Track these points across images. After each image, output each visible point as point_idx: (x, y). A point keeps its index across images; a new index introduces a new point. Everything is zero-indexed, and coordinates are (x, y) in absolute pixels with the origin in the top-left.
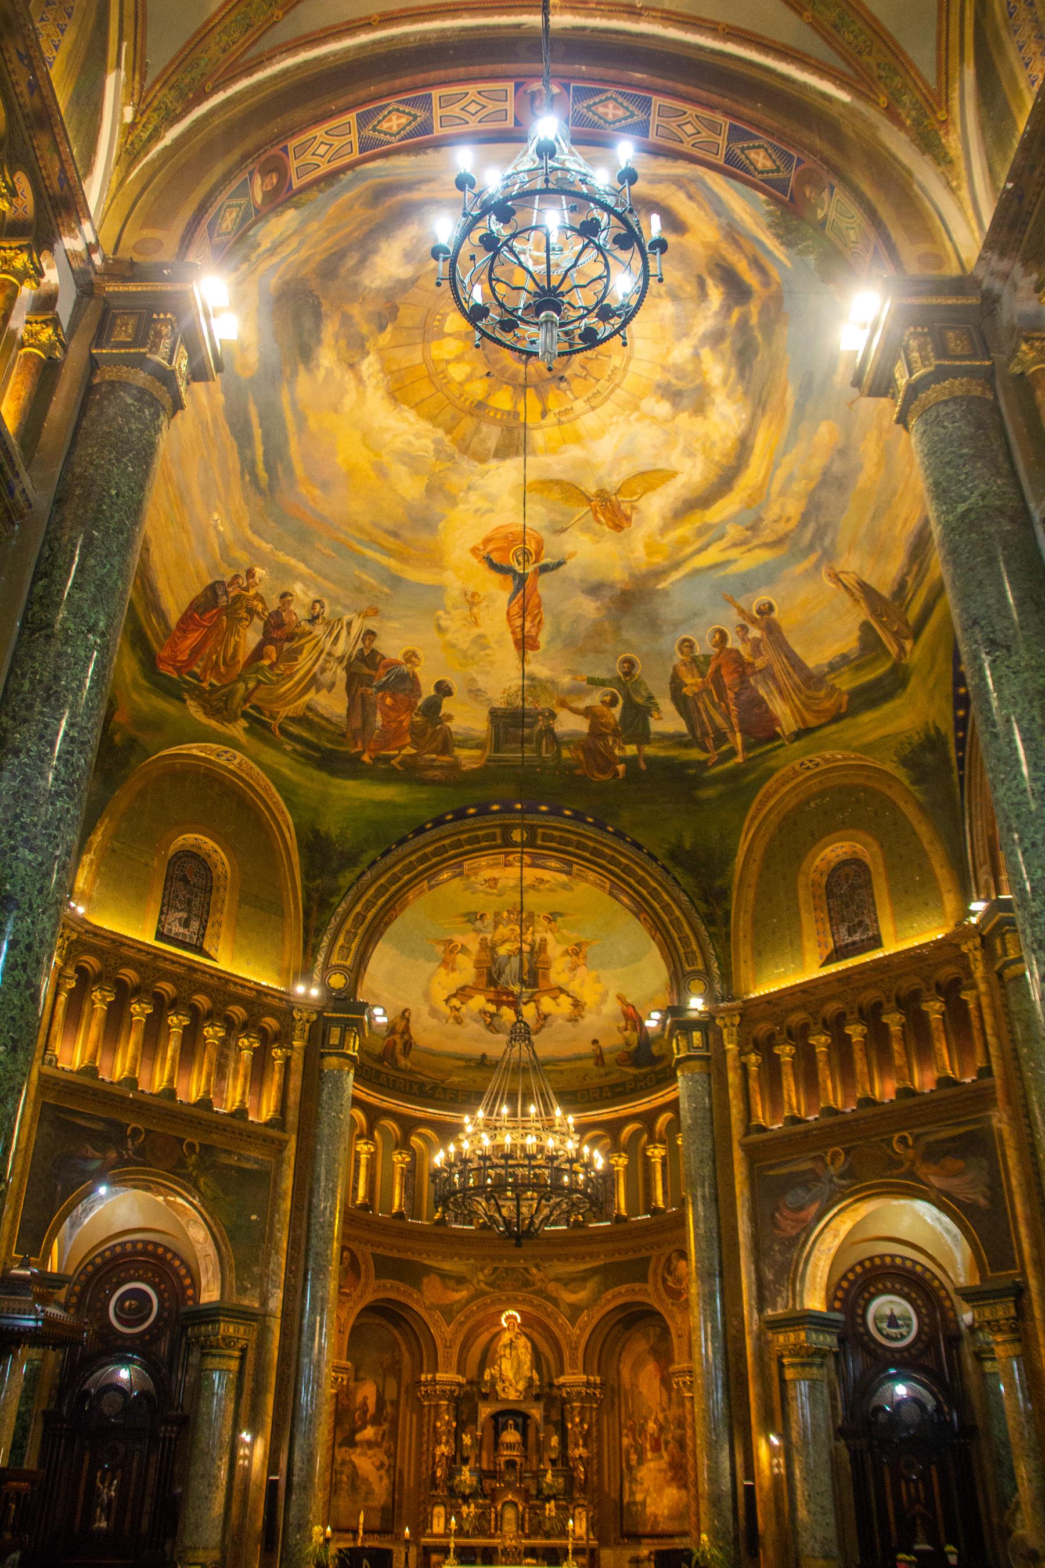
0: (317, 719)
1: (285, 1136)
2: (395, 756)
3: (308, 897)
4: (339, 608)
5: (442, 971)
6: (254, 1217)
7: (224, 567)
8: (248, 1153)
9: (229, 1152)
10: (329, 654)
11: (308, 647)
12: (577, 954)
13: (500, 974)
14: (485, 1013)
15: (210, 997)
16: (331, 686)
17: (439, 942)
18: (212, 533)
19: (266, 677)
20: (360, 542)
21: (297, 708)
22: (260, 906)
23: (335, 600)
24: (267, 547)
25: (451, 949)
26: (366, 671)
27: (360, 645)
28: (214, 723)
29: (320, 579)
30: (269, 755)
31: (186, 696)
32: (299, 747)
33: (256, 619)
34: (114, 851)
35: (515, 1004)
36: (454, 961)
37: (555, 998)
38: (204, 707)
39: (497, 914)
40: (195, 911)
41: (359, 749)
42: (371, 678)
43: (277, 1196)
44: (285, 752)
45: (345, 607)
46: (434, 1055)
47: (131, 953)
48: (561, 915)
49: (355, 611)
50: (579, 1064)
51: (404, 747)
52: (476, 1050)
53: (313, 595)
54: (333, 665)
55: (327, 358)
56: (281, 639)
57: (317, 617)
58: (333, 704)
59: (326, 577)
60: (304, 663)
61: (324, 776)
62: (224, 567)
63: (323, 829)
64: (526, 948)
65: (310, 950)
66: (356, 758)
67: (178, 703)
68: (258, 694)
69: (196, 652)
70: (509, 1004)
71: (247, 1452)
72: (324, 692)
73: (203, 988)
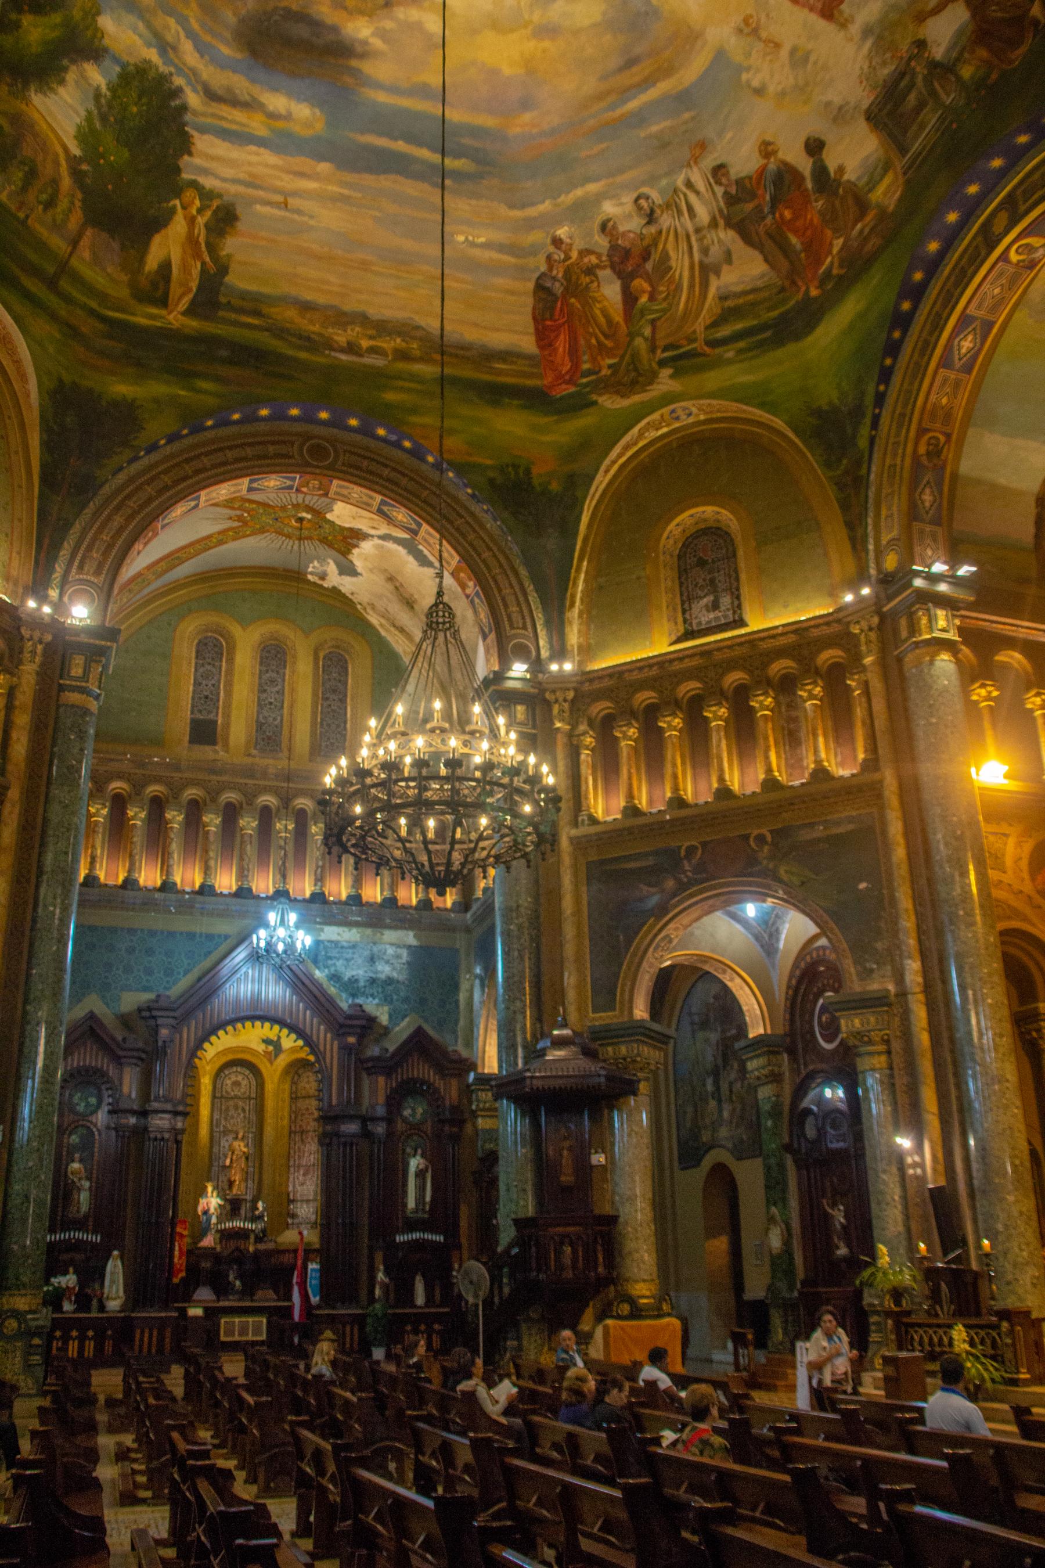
0: (741, 301)
1: (877, 776)
2: (832, 263)
3: (841, 486)
4: (664, 182)
6: (863, 886)
7: (531, 262)
8: (836, 816)
9: (812, 825)
10: (698, 230)
11: (670, 246)
15: (743, 668)
16: (728, 257)
18: (477, 252)
19: (657, 311)
20: (612, 107)
21: (711, 308)
22: (785, 536)
23: (652, 180)
24: (546, 206)
26: (749, 207)
27: (719, 191)
28: (636, 398)
29: (619, 179)
30: (713, 379)
31: (594, 397)
32: (741, 344)
33: (601, 273)
34: (601, 588)
38: (617, 392)
40: (721, 586)
41: (803, 289)
42: (759, 209)
43: (887, 848)
44: (730, 362)
45: (668, 174)
47: (636, 676)
49: (683, 167)
51: (831, 245)
53: (628, 199)
54: (711, 236)
55: (361, 30)
56: (639, 266)
57: (652, 211)
58: (746, 270)
59: (621, 171)
60: (681, 265)
61: (792, 347)
62: (531, 262)
63: (823, 403)
65: (857, 544)
66: (807, 299)
67: (592, 410)
68: (661, 334)
69: (573, 352)
71: (917, 1159)
72: (725, 268)
73: (731, 665)
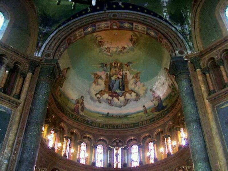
1: (19, 101)
5: (94, 85)
12: (137, 77)
13: (113, 86)
14: (108, 100)
17: (92, 74)
25: (98, 77)
35: (117, 96)
36: (98, 82)
37: (130, 94)
39: (111, 65)
46: (91, 112)
48: (131, 63)
50: (139, 114)
52: (105, 111)
64: (121, 77)
70: (116, 97)
